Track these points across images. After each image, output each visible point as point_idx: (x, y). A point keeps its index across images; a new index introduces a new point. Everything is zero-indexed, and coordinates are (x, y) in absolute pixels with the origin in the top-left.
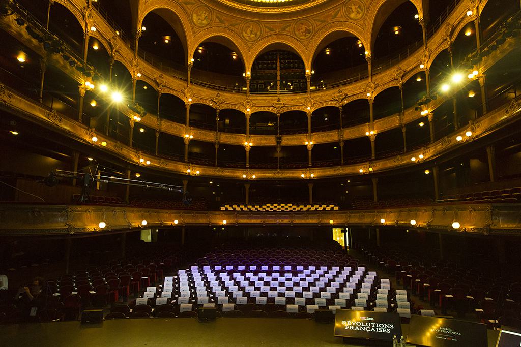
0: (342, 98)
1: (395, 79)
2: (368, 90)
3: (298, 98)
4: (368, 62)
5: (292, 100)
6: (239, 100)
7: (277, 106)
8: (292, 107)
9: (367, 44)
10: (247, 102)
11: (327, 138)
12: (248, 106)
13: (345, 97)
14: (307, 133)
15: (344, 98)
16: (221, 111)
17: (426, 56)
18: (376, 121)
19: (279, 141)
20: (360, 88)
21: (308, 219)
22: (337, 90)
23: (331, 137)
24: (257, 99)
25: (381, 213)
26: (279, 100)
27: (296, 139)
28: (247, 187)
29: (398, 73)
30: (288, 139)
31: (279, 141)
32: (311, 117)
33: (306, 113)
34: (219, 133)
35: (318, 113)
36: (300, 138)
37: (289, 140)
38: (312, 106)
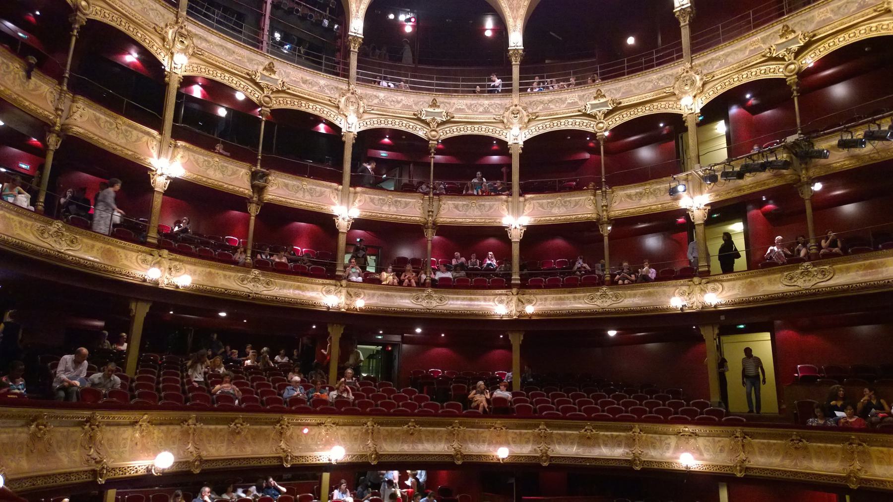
0: (439, 119)
1: (585, 115)
2: (513, 118)
3: (322, 82)
4: (513, 59)
5: (305, 82)
6: (152, 16)
7: (263, 83)
9: (515, 18)
10: (182, 35)
11: (393, 210)
12: (179, 46)
14: (340, 183)
15: (443, 123)
16: (90, 21)
17: (693, 82)
19: (258, 183)
20: (486, 111)
21: (420, 441)
22: (427, 98)
24: (206, 40)
25: (656, 433)
26: (270, 69)
27: (311, 192)
28: (140, 311)
29: (596, 102)
30: (286, 185)
31: (258, 183)
32: (354, 146)
34: (69, 96)
35: (369, 139)
36: (321, 194)
37: (285, 189)
38: (359, 117)
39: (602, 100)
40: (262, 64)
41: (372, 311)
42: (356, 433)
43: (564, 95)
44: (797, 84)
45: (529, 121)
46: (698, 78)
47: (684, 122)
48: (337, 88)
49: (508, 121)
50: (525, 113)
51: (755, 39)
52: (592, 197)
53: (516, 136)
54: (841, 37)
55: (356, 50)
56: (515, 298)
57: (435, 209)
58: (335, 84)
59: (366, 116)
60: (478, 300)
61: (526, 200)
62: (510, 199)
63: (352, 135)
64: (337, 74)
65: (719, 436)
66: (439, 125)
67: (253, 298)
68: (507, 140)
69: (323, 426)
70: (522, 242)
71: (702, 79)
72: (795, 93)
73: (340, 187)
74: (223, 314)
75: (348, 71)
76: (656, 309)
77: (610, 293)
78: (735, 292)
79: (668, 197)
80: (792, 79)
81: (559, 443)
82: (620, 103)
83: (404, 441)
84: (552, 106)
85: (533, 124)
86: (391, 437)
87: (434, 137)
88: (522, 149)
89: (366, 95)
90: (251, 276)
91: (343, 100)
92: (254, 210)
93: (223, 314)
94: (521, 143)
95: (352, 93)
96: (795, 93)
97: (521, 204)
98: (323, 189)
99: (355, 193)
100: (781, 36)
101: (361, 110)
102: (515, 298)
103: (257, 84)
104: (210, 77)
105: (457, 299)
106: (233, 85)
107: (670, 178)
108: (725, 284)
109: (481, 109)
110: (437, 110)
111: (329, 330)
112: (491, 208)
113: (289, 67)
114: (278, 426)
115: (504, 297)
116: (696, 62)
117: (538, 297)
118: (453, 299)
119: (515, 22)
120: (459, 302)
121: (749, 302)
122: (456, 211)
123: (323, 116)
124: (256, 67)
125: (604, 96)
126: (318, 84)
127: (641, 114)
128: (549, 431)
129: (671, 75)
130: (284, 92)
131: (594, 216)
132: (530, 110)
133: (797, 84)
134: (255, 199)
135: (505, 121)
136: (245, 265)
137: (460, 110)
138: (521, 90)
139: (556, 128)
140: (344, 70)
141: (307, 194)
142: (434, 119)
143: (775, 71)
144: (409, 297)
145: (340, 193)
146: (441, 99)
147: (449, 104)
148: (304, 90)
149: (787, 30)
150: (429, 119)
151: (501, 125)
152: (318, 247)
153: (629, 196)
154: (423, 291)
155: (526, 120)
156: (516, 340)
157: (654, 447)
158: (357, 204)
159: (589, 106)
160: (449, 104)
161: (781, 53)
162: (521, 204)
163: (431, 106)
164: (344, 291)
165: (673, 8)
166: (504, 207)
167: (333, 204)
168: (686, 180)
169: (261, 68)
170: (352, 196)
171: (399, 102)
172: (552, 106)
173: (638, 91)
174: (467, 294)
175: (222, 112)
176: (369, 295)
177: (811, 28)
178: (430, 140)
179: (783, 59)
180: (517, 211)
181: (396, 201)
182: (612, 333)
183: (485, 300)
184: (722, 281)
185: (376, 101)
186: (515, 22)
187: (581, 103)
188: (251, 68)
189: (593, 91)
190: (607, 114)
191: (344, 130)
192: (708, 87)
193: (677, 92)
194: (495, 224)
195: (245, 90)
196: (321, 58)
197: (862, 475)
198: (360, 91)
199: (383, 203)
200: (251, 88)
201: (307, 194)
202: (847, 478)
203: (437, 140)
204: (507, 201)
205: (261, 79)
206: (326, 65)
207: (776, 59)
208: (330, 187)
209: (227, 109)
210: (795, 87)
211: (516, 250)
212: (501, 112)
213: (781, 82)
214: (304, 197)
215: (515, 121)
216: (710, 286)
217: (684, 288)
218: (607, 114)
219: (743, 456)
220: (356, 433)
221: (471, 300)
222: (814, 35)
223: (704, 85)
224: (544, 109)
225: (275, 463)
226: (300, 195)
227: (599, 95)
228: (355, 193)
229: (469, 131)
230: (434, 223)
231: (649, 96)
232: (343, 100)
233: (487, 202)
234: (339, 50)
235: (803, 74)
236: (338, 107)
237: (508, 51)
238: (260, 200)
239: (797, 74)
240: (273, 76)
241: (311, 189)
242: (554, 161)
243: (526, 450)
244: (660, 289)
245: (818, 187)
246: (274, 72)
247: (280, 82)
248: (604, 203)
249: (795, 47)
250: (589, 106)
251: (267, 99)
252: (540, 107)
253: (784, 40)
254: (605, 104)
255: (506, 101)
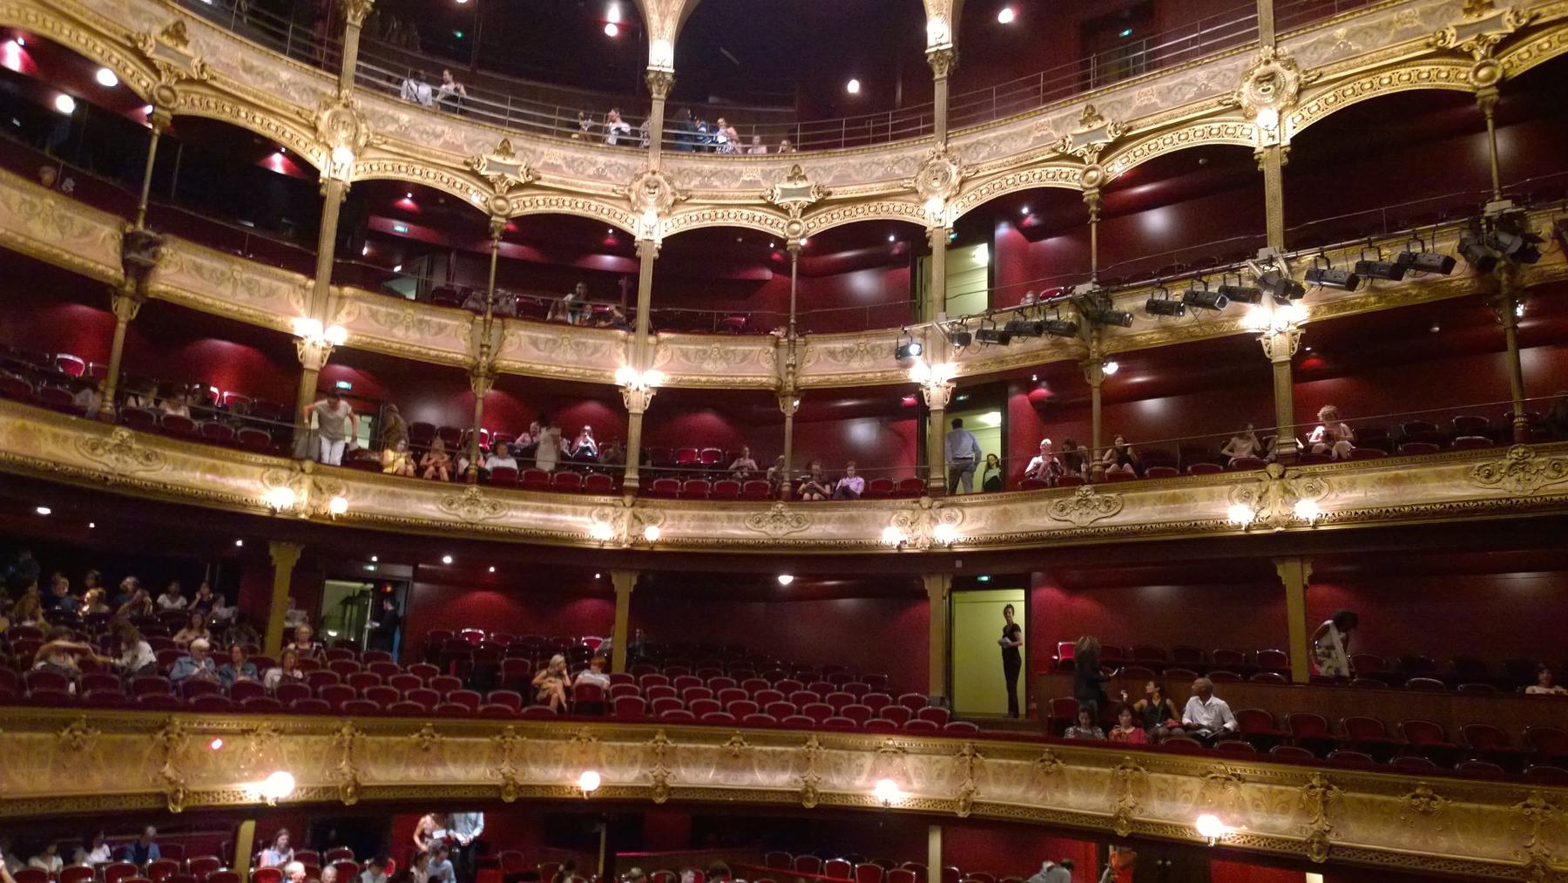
0: (512, 178)
1: (770, 205)
2: (647, 195)
3: (285, 75)
4: (655, 88)
5: (249, 70)
7: (159, 60)
8: (243, 111)
9: (663, 16)
13: (527, 186)
14: (311, 272)
15: (520, 187)
17: (946, 177)
18: (663, 336)
20: (599, 176)
21: (441, 761)
22: (493, 136)
23: (742, 363)
25: (843, 748)
26: (177, 33)
27: (249, 287)
29: (790, 185)
32: (343, 206)
33: (317, 172)
35: (372, 197)
36: (271, 292)
37: (190, 275)
38: (358, 153)
39: (801, 184)
40: (159, 21)
41: (362, 520)
42: (318, 748)
43: (737, 167)
44: (1098, 203)
45: (675, 203)
46: (954, 169)
47: (927, 240)
48: (314, 91)
49: (638, 198)
50: (668, 189)
51: (1043, 120)
52: (772, 349)
53: (652, 227)
54: (1168, 136)
55: (358, 23)
56: (628, 513)
57: (494, 342)
58: (311, 82)
59: (370, 154)
60: (562, 512)
61: (659, 342)
62: (632, 337)
63: (340, 188)
64: (316, 64)
65: (937, 753)
66: (511, 189)
67: (116, 485)
68: (633, 231)
69: (252, 736)
70: (647, 415)
71: (960, 173)
72: (1093, 218)
73: (311, 283)
74: (44, 511)
75: (339, 61)
76: (860, 546)
77: (788, 513)
78: (981, 524)
79: (892, 362)
80: (1092, 194)
81: (687, 765)
82: (830, 194)
83: (411, 762)
84: (716, 183)
85: (681, 209)
86: (387, 755)
87: (501, 209)
88: (659, 251)
89: (374, 113)
90: (113, 440)
91: (326, 116)
92: (124, 311)
93: (44, 511)
94: (658, 242)
95: (346, 106)
96: (1093, 218)
97: (651, 349)
98: (275, 284)
99: (341, 297)
100: (1083, 122)
101: (362, 142)
102: (628, 513)
103: (148, 62)
104: (47, 33)
105: (525, 508)
106: (95, 56)
107: (898, 330)
108: (968, 511)
109: (591, 171)
110: (509, 161)
111: (273, 551)
112: (596, 349)
113: (216, 35)
114: (160, 736)
115: (608, 510)
116: (953, 144)
117: (668, 512)
118: (516, 508)
119: (663, 22)
120: (527, 514)
121: (1000, 542)
122: (533, 350)
123: (283, 140)
124: (146, 26)
125: (804, 178)
126: (274, 77)
127: (861, 217)
128: (671, 744)
129: (914, 159)
130: (202, 83)
131: (773, 381)
132: (678, 184)
133: (1098, 203)
134: (128, 288)
135: (633, 197)
136: (99, 417)
137: (554, 168)
138: (664, 146)
139: (720, 223)
140: (331, 58)
141: (240, 289)
142: (502, 177)
143: (1068, 178)
144: (434, 500)
145: (309, 295)
146: (518, 141)
147: (534, 152)
148: (248, 85)
149: (1091, 115)
150: (492, 175)
151: (624, 204)
152: (266, 397)
153: (832, 353)
154: (463, 490)
155: (670, 202)
156: (624, 584)
157: (838, 772)
158: (343, 317)
159: (778, 191)
160: (534, 152)
161: (1081, 149)
162: (651, 349)
163: (497, 152)
164: (307, 481)
165: (925, 47)
166: (621, 351)
167: (295, 314)
168: (924, 336)
169: (157, 30)
170: (333, 302)
171: (437, 136)
172: (716, 183)
173: (860, 178)
174: (542, 500)
175: (65, 104)
176: (357, 491)
177: (1126, 115)
178: (492, 214)
179: (1081, 160)
180: (642, 359)
181: (421, 322)
182: (785, 580)
183: (575, 513)
184: (963, 505)
185: (392, 128)
186: (663, 22)
187: (769, 185)
188: (136, 26)
189: (786, 166)
190: (807, 210)
191: (324, 174)
192: (968, 186)
193: (920, 189)
194: (602, 380)
195: (118, 69)
196: (285, 27)
197: (1136, 816)
198: (360, 103)
199: (395, 321)
200: (132, 66)
201: (240, 289)
202: (1115, 820)
203: (507, 217)
204: (626, 341)
205: (156, 51)
206: (294, 43)
207: (1072, 158)
208: (290, 281)
209: (76, 100)
210: (1093, 208)
211: (635, 429)
212: (628, 180)
213: (1073, 196)
214: (234, 293)
215: (651, 200)
216: (946, 512)
217: (906, 513)
218: (807, 210)
219: (970, 784)
220: (318, 748)
221: (549, 511)
222: (1130, 129)
223: (962, 182)
224: (702, 185)
225: (152, 804)
226: (226, 290)
227: (796, 175)
228: (341, 297)
229: (566, 206)
230: (491, 369)
231: (877, 189)
232: (326, 116)
233: (591, 339)
234: (322, 18)
235: (1108, 189)
236: (315, 129)
237: (647, 72)
238: (140, 291)
239: (1099, 186)
240: (181, 49)
241: (250, 281)
242: (711, 279)
243: (630, 776)
244: (869, 513)
245: (1111, 368)
246: (186, 43)
247: (196, 62)
248: (791, 360)
249: (1100, 144)
250: (778, 191)
251: (166, 93)
252: (696, 182)
253: (1085, 129)
254: (804, 192)
255: (637, 163)
